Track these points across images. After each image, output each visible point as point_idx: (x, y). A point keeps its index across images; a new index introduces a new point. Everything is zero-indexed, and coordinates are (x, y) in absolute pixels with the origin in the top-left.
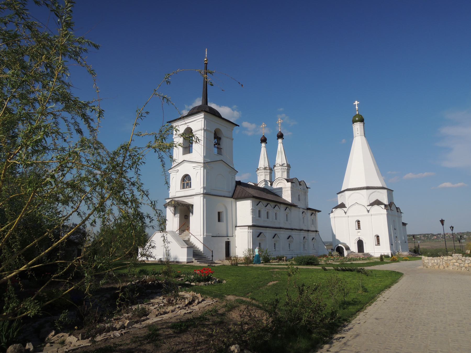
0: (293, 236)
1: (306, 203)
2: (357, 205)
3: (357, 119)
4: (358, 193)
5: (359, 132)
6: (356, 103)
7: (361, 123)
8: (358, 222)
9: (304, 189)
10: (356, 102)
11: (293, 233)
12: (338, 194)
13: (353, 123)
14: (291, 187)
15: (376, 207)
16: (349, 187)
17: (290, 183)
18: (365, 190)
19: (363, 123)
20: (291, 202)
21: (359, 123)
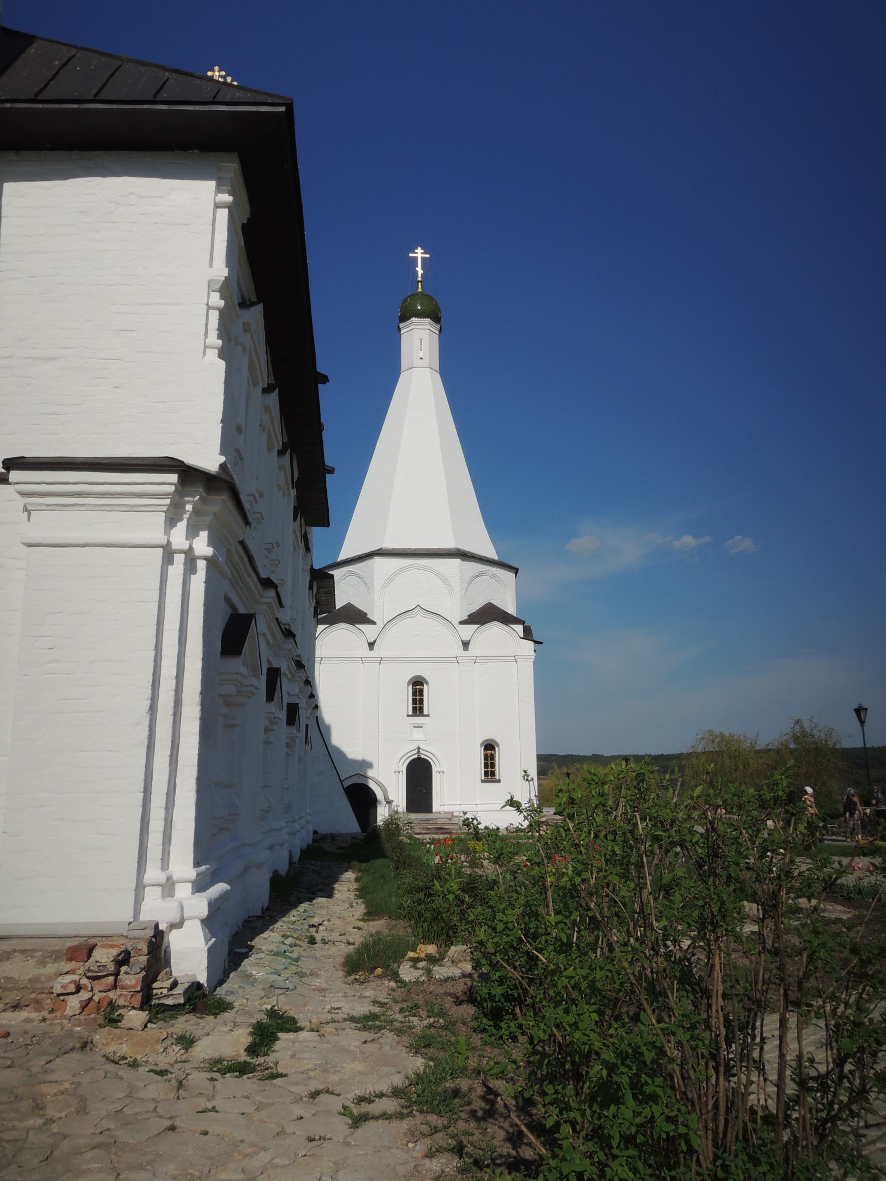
2: (419, 618)
4: (425, 569)
6: (419, 254)
7: (433, 324)
8: (418, 684)
10: (419, 248)
15: (495, 628)
18: (457, 561)
21: (428, 320)
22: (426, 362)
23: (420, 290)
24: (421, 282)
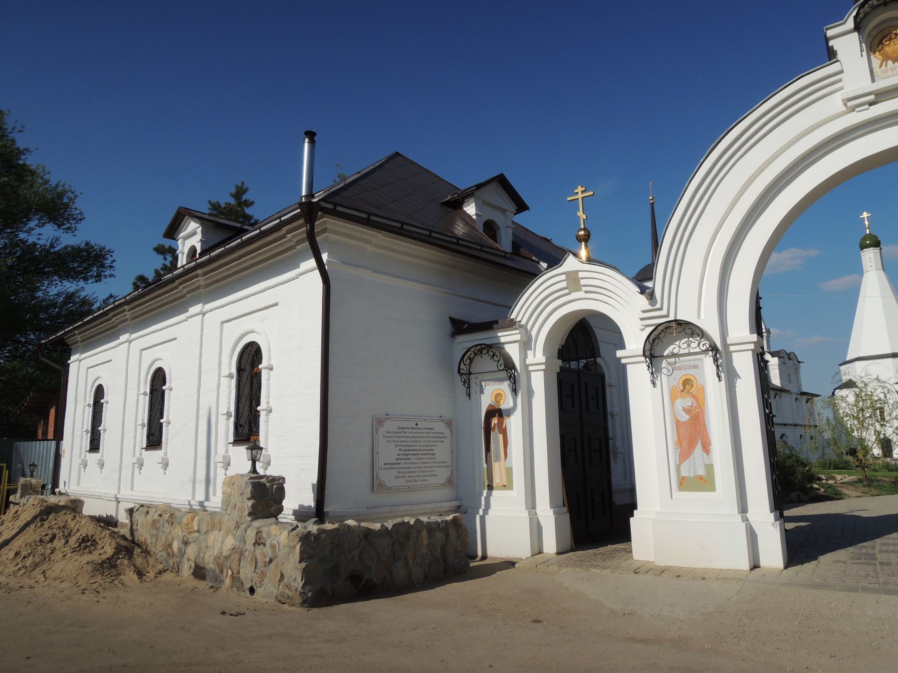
0: (787, 434)
1: (799, 385)
3: (868, 242)
4: (877, 364)
5: (873, 264)
6: (865, 215)
9: (794, 365)
11: (787, 430)
12: (841, 365)
13: (862, 249)
14: (779, 364)
16: (862, 355)
17: (777, 358)
18: (891, 359)
19: (879, 248)
20: (780, 386)
21: (872, 248)
22: (874, 267)
23: (868, 232)
24: (868, 228)
